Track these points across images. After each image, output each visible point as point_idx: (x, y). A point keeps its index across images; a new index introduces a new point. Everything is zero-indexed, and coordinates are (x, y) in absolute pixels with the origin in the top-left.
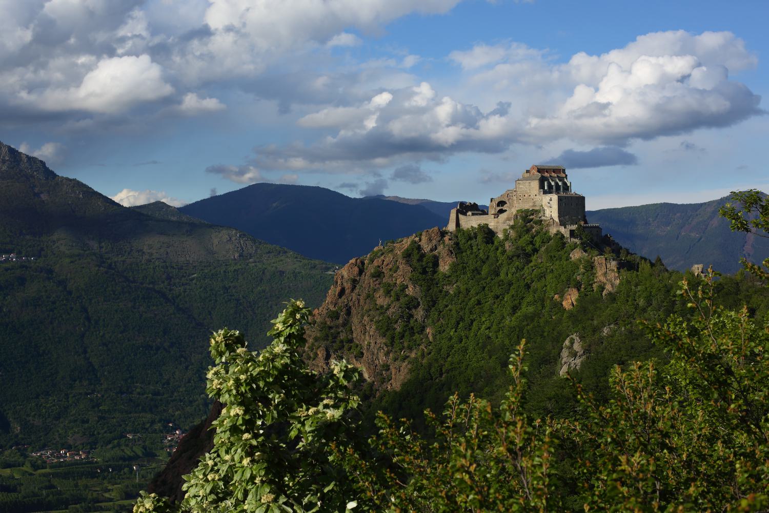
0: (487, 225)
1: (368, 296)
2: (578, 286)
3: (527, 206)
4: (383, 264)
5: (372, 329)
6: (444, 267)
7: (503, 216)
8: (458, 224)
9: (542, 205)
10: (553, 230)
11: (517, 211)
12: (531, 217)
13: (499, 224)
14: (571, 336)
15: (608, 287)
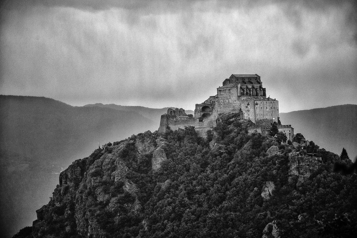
1: (89, 194)
2: (273, 179)
3: (227, 111)
4: (102, 164)
5: (93, 223)
6: (157, 165)
9: (241, 109)
11: (220, 115)
12: (231, 120)
13: (203, 128)
14: (270, 223)
15: (301, 180)
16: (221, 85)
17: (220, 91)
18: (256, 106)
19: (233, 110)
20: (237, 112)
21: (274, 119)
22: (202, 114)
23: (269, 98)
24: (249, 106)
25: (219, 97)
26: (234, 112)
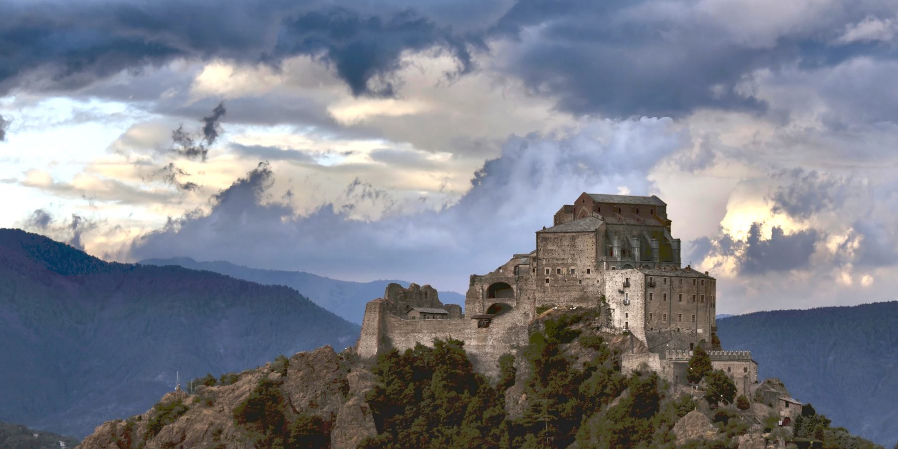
0: (462, 344)
3: (564, 302)
7: (500, 325)
8: (384, 340)
9: (603, 298)
10: (630, 364)
12: (574, 328)
13: (487, 346)
16: (550, 223)
17: (545, 239)
18: (650, 291)
19: (582, 299)
20: (591, 305)
21: (700, 331)
22: (489, 303)
23: (689, 268)
24: (627, 291)
25: (541, 256)
26: (584, 305)
